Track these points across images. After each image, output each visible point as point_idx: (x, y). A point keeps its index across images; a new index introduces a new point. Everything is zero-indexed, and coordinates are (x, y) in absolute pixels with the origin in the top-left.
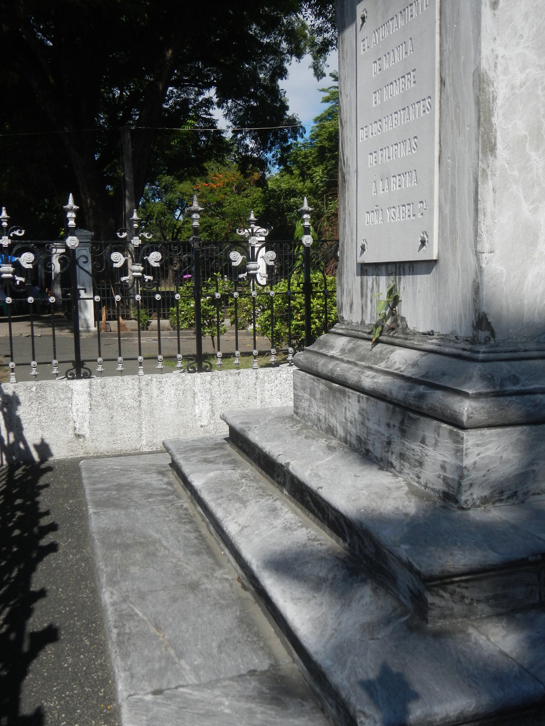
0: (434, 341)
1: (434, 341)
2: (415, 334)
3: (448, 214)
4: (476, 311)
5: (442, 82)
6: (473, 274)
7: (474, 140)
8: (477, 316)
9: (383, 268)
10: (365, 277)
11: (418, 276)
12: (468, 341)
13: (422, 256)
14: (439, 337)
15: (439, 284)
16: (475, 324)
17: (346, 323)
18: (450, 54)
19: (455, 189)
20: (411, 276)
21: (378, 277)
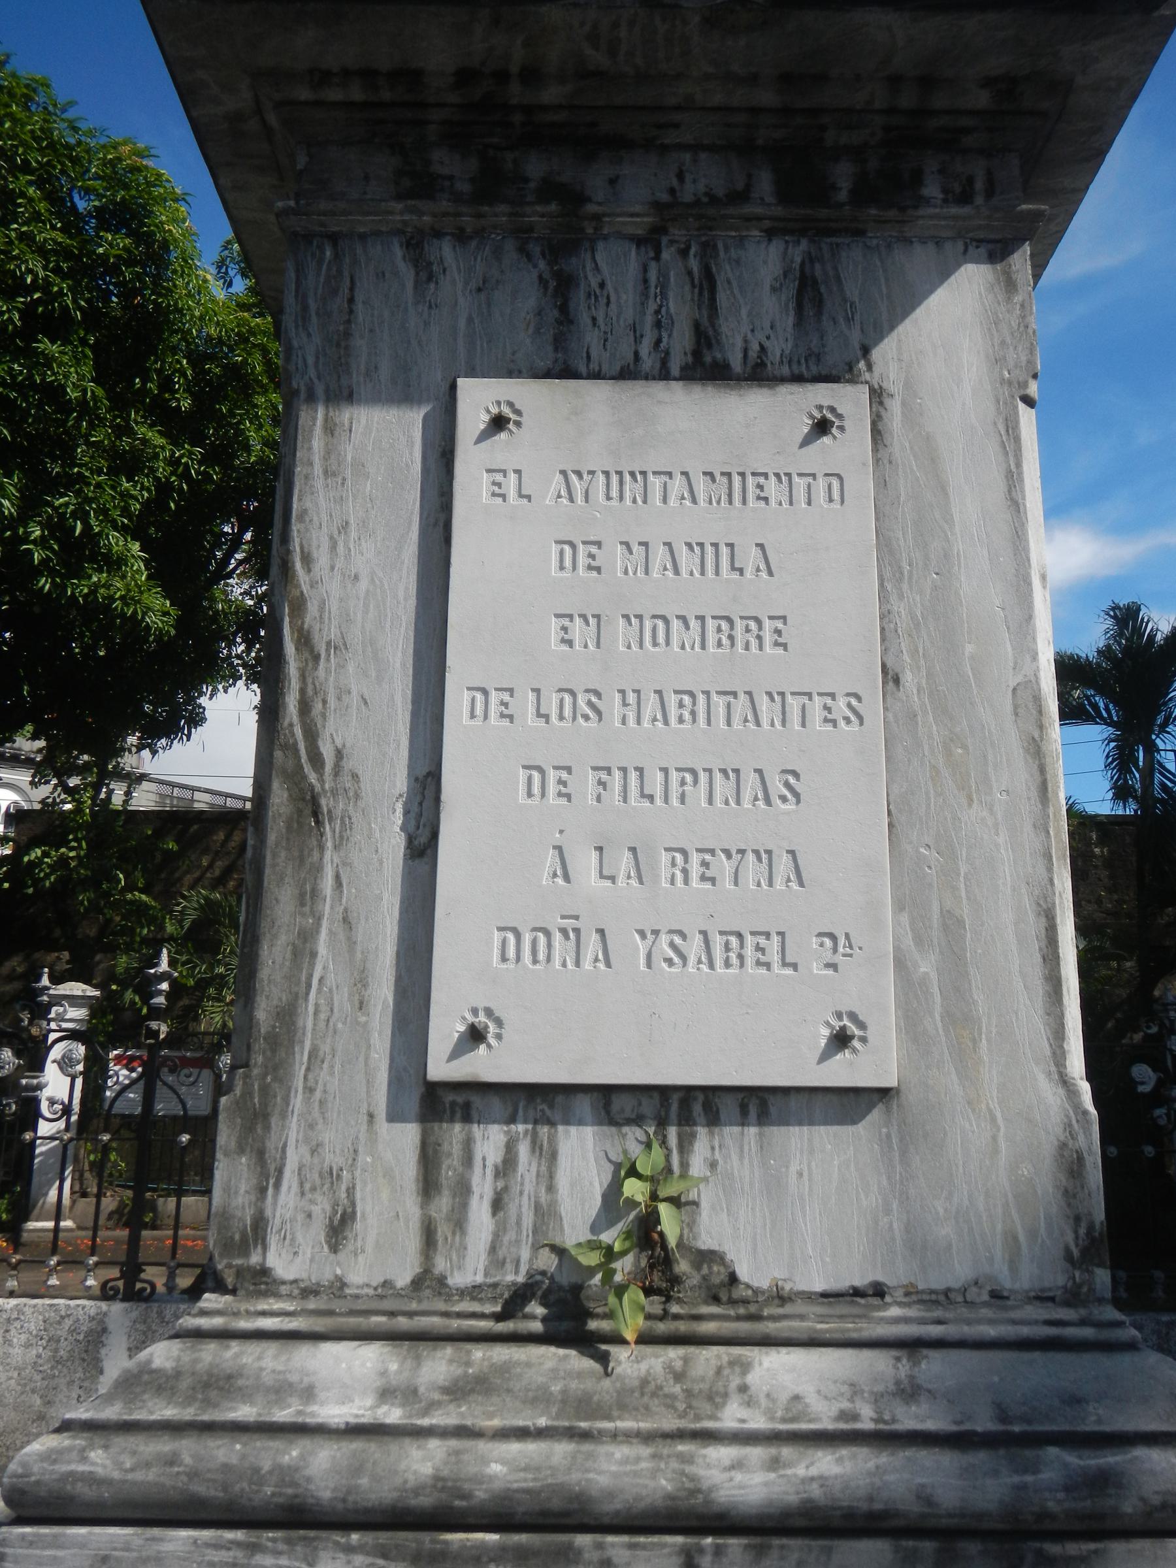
0: (895, 1312)
1: (895, 1312)
2: (781, 1297)
3: (934, 976)
4: (1077, 1219)
5: (891, 678)
6: (1059, 1130)
7: (1028, 828)
8: (1082, 1231)
9: (584, 1105)
10: (458, 1127)
11: (795, 1130)
12: (1052, 1299)
13: (842, 1072)
14: (914, 1298)
15: (904, 1153)
16: (1076, 1252)
17: (284, 1289)
18: (917, 625)
19: (961, 923)
20: (752, 1131)
21: (544, 1130)
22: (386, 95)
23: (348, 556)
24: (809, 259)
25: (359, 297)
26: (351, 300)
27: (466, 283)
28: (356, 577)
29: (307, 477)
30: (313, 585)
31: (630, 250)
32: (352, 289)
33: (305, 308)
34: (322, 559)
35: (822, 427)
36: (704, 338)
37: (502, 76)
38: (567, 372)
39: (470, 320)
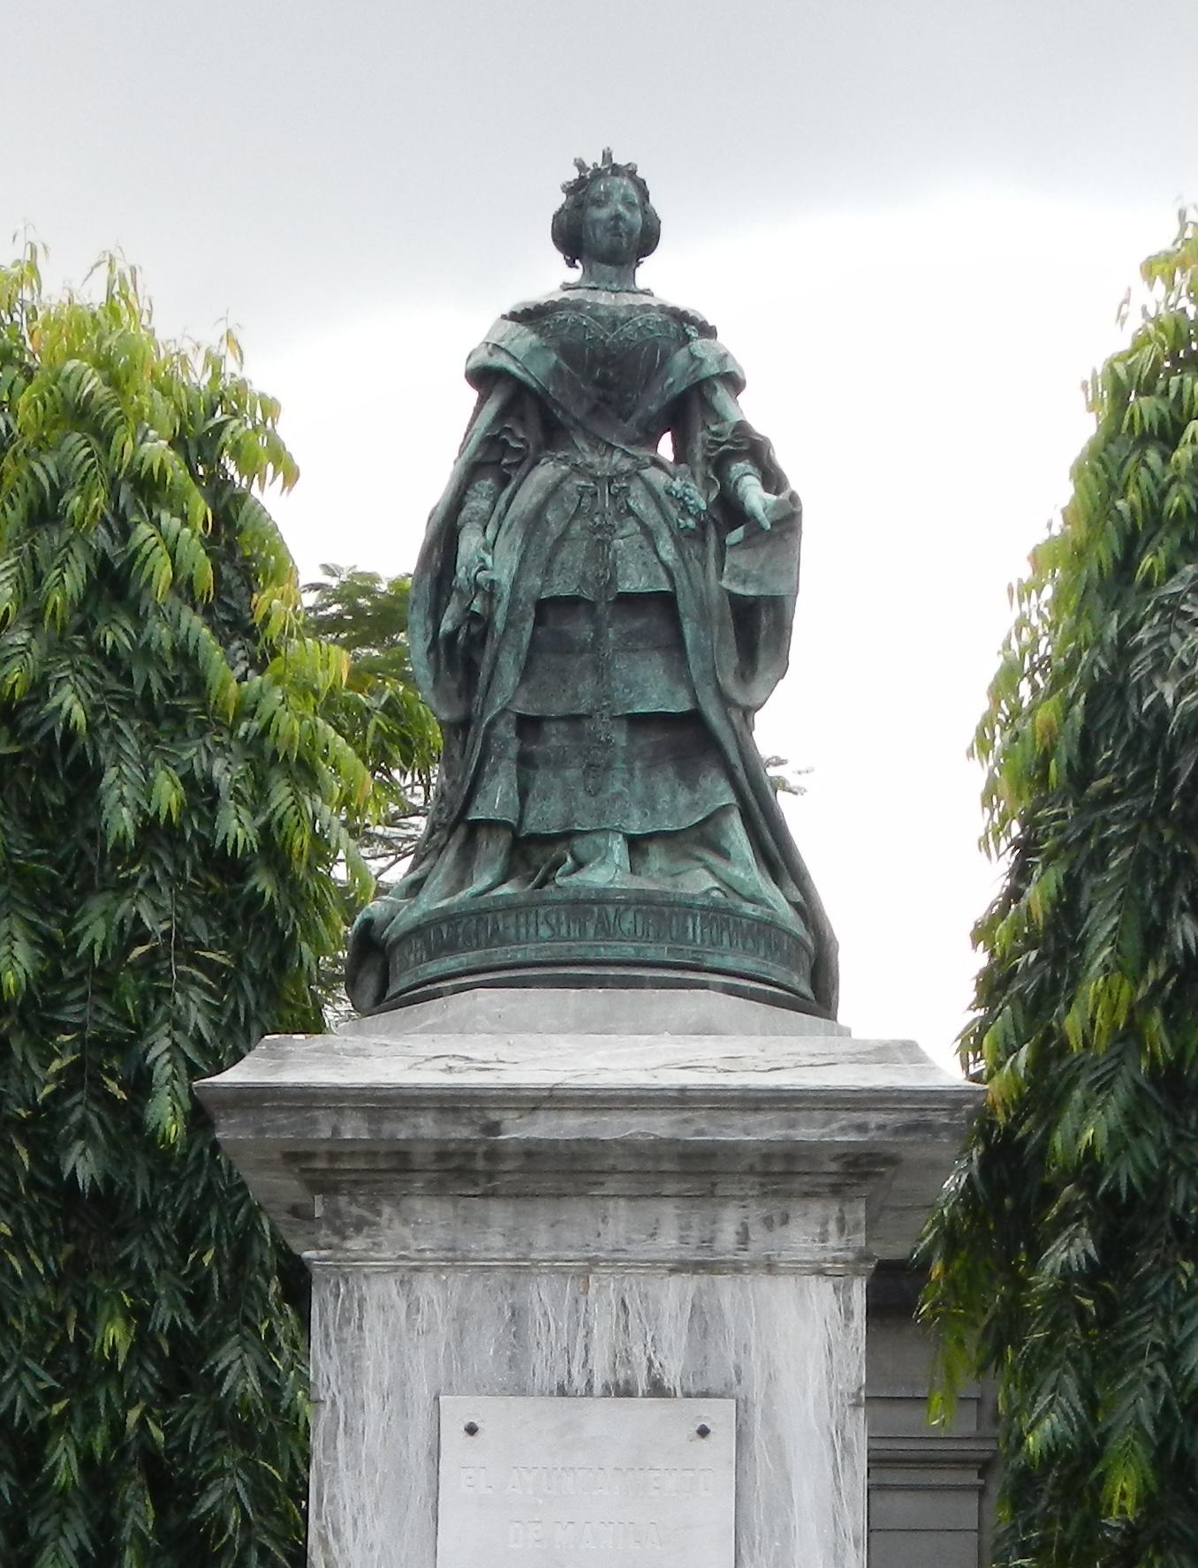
22: (383, 1166)
23: (365, 1531)
24: (699, 1292)
25: (366, 1326)
26: (360, 1328)
27: (445, 1313)
28: (372, 1547)
29: (334, 1471)
30: (341, 1551)
31: (563, 1291)
32: (360, 1319)
33: (327, 1335)
34: (348, 1532)
35: (703, 1432)
36: (622, 1357)
37: (470, 1155)
38: (522, 1391)
39: (448, 1344)
